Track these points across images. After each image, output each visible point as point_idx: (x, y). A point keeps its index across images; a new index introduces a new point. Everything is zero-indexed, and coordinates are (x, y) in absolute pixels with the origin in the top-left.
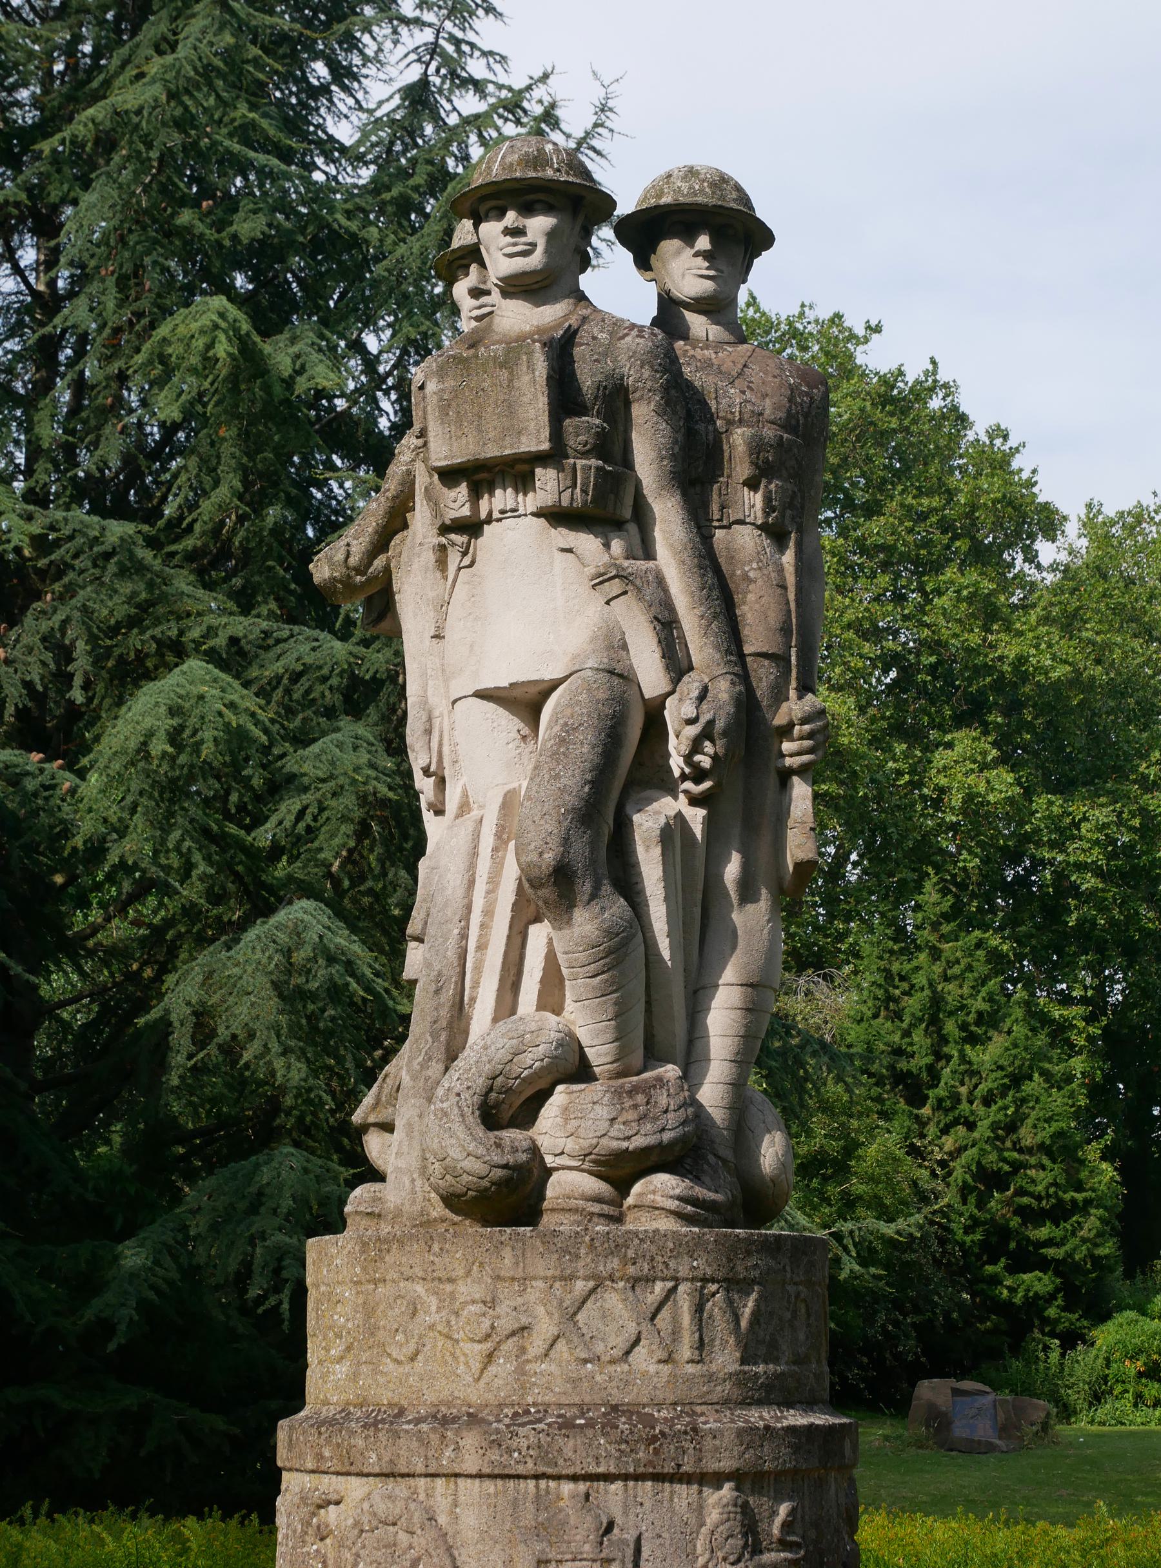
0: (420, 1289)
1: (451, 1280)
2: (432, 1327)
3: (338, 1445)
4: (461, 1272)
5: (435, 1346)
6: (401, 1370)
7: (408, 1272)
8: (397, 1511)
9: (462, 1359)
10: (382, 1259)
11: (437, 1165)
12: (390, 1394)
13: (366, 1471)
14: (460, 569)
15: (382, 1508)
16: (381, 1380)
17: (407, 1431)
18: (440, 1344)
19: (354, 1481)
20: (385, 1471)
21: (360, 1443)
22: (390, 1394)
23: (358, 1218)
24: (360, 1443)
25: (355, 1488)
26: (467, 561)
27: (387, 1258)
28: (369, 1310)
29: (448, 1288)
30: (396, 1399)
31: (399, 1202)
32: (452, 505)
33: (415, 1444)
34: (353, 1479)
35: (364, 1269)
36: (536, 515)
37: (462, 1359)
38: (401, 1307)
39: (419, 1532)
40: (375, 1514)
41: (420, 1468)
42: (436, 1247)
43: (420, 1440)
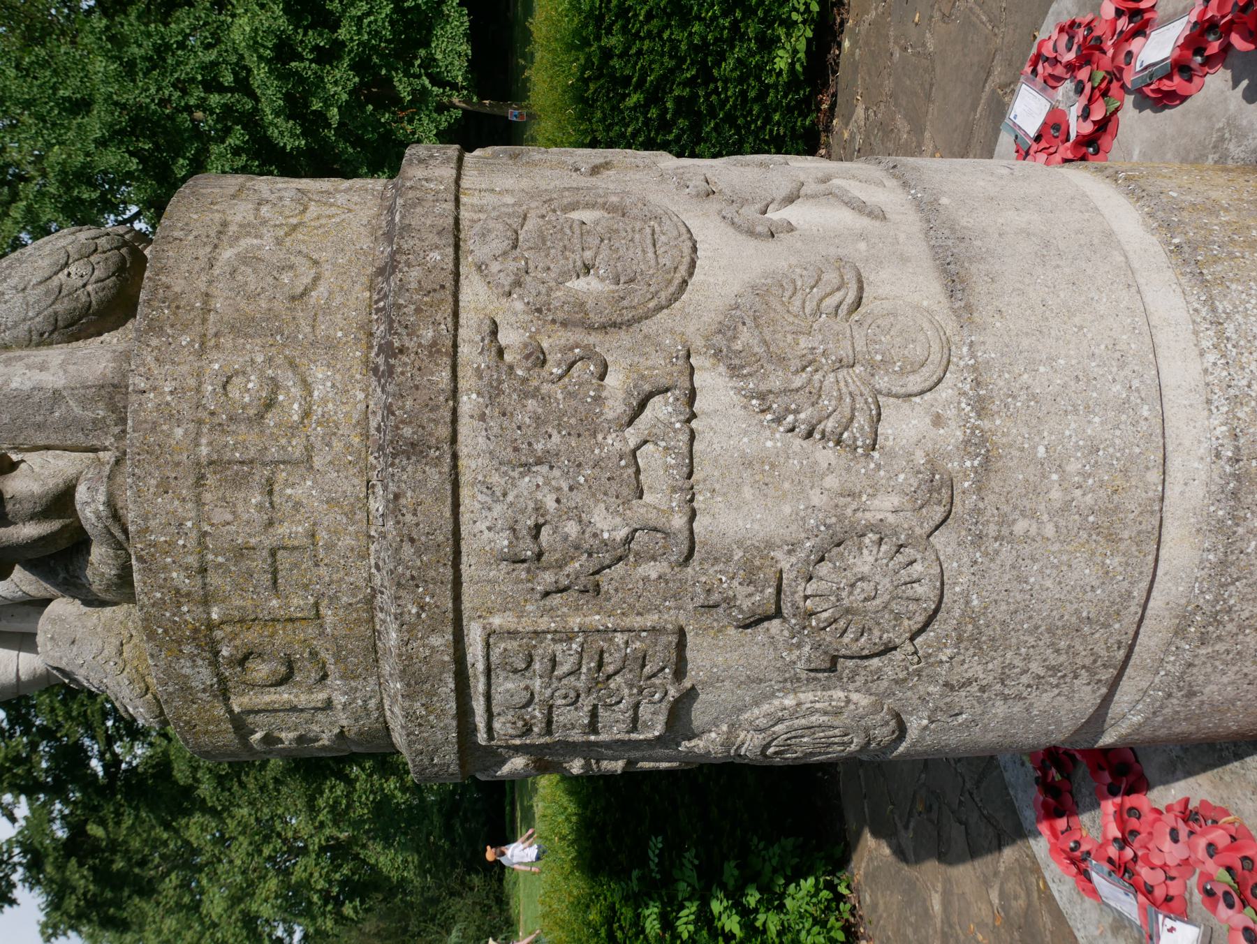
0: (227, 254)
1: (225, 224)
2: (279, 242)
3: (418, 310)
4: (217, 216)
5: (304, 242)
6: (327, 274)
7: (203, 262)
8: (500, 227)
9: (323, 221)
10: (177, 296)
11: (72, 269)
12: (358, 287)
13: (451, 266)
15: (498, 244)
16: (338, 299)
17: (403, 217)
18: (300, 237)
19: (466, 296)
20: (451, 241)
21: (415, 273)
22: (358, 287)
23: (119, 479)
24: (415, 273)
25: (475, 295)
27: (177, 289)
28: (241, 327)
29: (233, 228)
30: (365, 280)
31: (109, 355)
33: (419, 210)
34: (462, 297)
35: (186, 327)
37: (323, 221)
38: (248, 276)
39: (524, 207)
40: (505, 253)
41: (450, 206)
42: (176, 234)
43: (414, 206)
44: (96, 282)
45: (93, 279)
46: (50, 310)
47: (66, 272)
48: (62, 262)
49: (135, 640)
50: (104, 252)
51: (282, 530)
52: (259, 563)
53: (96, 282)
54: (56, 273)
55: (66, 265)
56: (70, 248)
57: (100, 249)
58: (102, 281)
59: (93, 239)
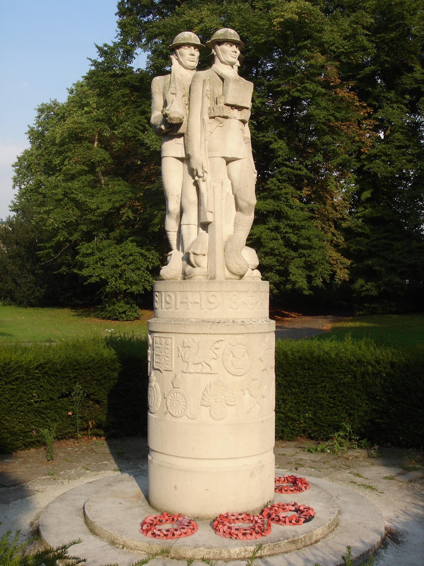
26: (221, 125)
51: (190, 305)
52: (185, 301)
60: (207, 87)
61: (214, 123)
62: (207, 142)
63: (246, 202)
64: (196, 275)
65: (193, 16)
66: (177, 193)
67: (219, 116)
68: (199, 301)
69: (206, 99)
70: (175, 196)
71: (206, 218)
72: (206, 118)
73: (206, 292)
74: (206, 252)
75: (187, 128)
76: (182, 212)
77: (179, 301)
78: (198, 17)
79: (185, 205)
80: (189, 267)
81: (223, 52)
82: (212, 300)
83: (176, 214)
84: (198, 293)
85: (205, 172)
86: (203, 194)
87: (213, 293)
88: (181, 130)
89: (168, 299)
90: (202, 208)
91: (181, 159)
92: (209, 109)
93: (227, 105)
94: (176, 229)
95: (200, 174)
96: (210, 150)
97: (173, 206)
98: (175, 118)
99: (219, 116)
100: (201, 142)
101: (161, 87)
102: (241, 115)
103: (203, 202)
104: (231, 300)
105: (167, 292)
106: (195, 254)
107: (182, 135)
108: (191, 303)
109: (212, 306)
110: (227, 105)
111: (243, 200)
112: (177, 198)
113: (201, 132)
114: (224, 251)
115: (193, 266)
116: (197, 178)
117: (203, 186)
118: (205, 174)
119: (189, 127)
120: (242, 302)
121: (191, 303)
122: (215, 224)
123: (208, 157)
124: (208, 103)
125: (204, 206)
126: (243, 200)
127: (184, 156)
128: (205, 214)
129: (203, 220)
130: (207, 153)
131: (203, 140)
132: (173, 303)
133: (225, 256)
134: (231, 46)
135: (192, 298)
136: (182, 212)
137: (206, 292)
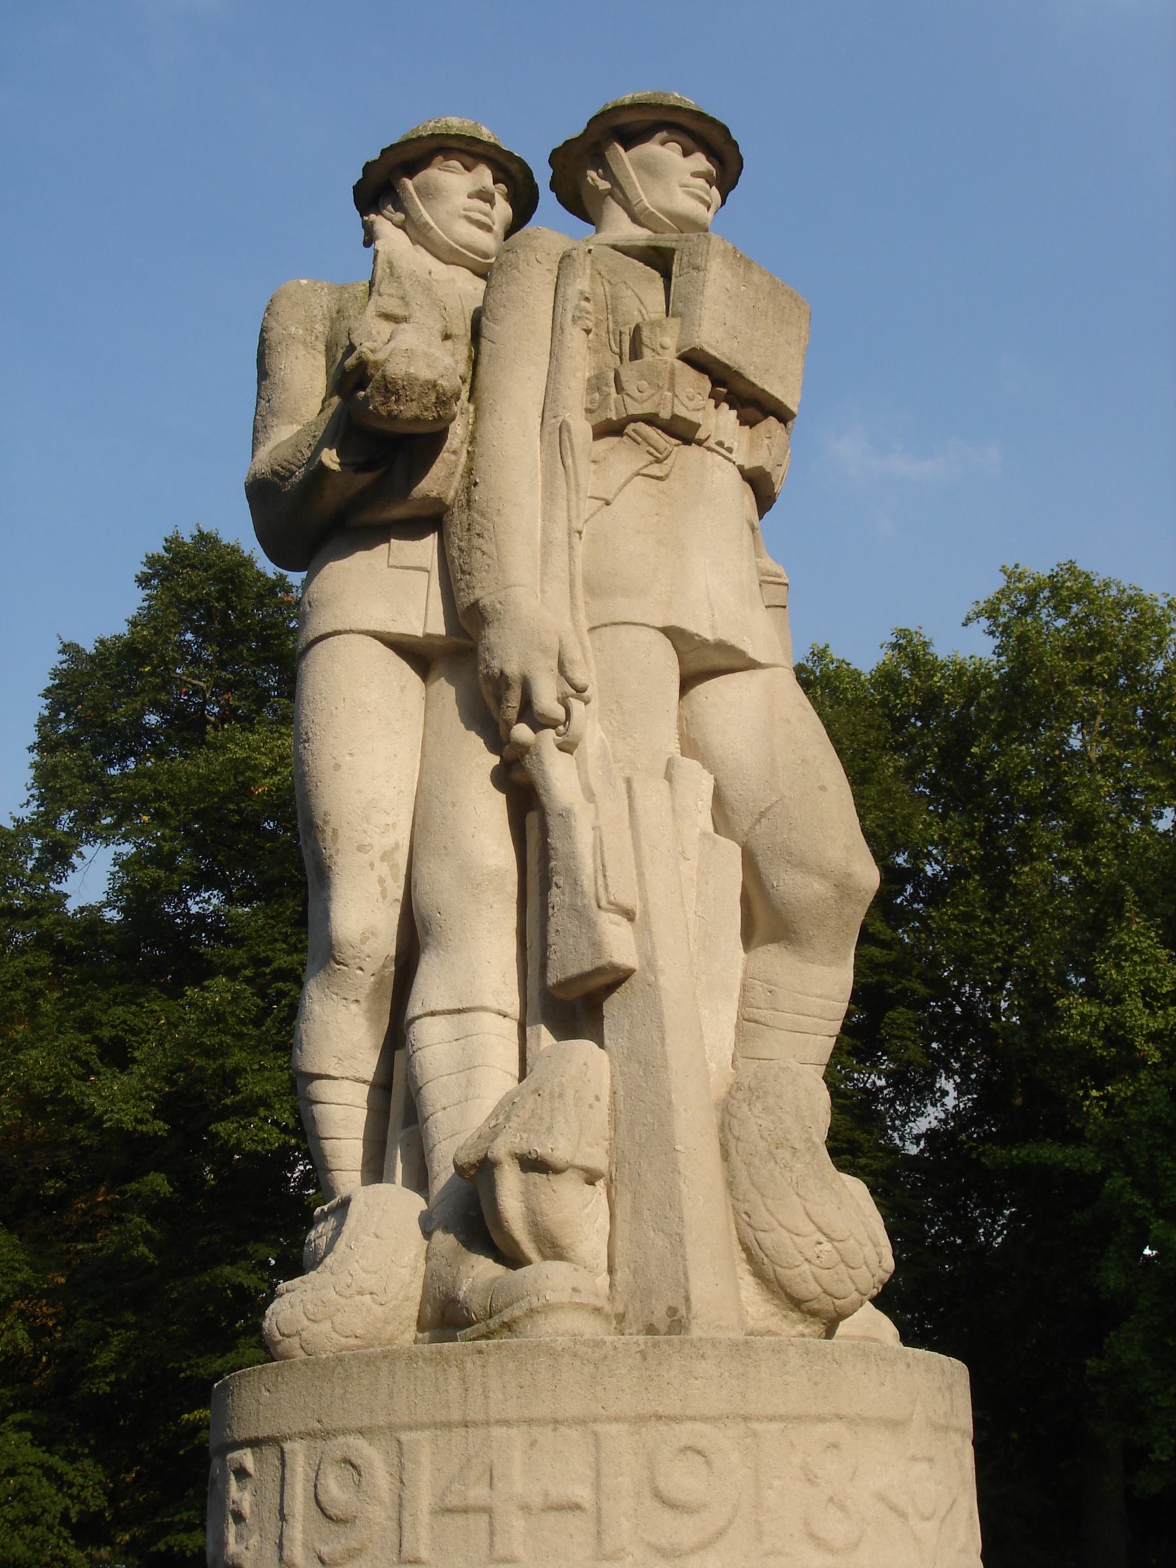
11: (827, 1246)
14: (638, 474)
26: (655, 470)
32: (686, 402)
36: (741, 469)
44: (813, 1274)
45: (815, 1270)
46: (775, 1224)
47: (823, 1239)
48: (833, 1235)
49: (378, 1310)
50: (851, 1278)
51: (518, 1524)
52: (478, 1493)
53: (813, 1274)
54: (820, 1229)
55: (830, 1239)
56: (852, 1242)
57: (852, 1272)
58: (816, 1279)
59: (866, 1263)
60: (581, 283)
61: (622, 458)
62: (580, 548)
63: (823, 875)
64: (549, 1308)
65: (257, 749)
66: (388, 841)
67: (651, 420)
68: (582, 1493)
69: (575, 340)
70: (375, 854)
71: (596, 946)
72: (581, 428)
73: (641, 1420)
74: (599, 1160)
75: (469, 471)
76: (412, 940)
77: (424, 1498)
78: (271, 751)
79: (441, 889)
80: (481, 1270)
81: (650, 169)
82: (683, 1480)
83: (372, 966)
84: (573, 1433)
85: (580, 691)
86: (566, 815)
87: (685, 1433)
88: (439, 481)
89: (335, 1490)
90: (555, 896)
91: (418, 655)
92: (595, 384)
93: (696, 360)
94: (368, 1065)
95: (547, 699)
96: (594, 590)
97: (361, 913)
98: (411, 380)
99: (651, 420)
100: (547, 544)
101: (318, 312)
102: (753, 445)
103: (572, 855)
104: (811, 1479)
105: (327, 1435)
106: (533, 1164)
107: (431, 520)
108: (526, 1508)
109: (685, 1530)
110: (696, 360)
111: (802, 865)
112: (383, 869)
113: (549, 496)
114: (725, 1155)
115: (512, 1259)
116: (522, 732)
117: (560, 776)
118: (576, 705)
119: (481, 463)
120: (882, 1498)
121: (526, 1508)
122: (653, 986)
123: (585, 625)
124: (581, 362)
125: (575, 883)
126: (802, 865)
127: (438, 627)
128: (591, 925)
129: (568, 961)
130: (580, 602)
131: (559, 534)
132: (379, 1514)
133: (731, 1185)
134: (686, 153)
135: (530, 1469)
136: (412, 940)
137: (641, 1420)
